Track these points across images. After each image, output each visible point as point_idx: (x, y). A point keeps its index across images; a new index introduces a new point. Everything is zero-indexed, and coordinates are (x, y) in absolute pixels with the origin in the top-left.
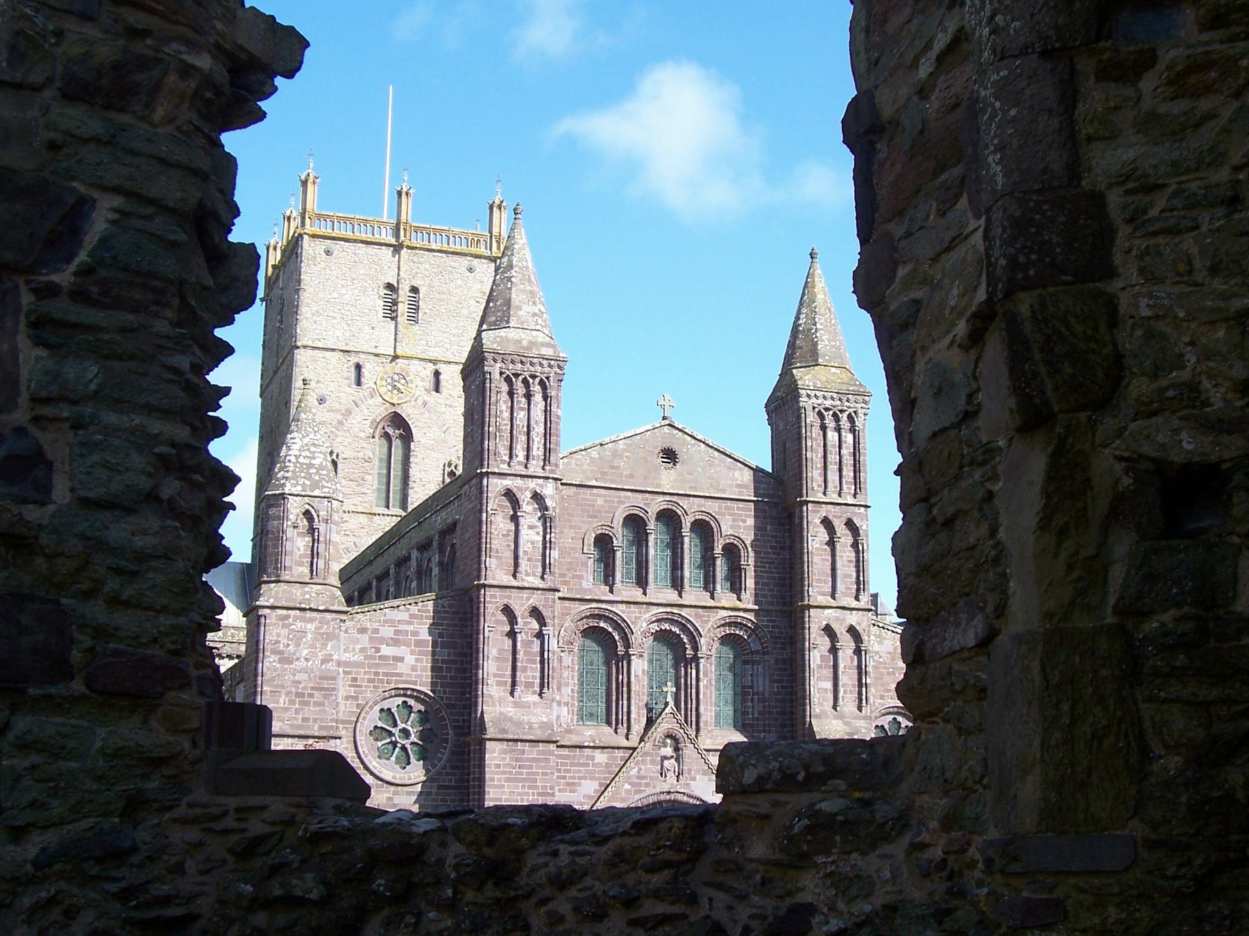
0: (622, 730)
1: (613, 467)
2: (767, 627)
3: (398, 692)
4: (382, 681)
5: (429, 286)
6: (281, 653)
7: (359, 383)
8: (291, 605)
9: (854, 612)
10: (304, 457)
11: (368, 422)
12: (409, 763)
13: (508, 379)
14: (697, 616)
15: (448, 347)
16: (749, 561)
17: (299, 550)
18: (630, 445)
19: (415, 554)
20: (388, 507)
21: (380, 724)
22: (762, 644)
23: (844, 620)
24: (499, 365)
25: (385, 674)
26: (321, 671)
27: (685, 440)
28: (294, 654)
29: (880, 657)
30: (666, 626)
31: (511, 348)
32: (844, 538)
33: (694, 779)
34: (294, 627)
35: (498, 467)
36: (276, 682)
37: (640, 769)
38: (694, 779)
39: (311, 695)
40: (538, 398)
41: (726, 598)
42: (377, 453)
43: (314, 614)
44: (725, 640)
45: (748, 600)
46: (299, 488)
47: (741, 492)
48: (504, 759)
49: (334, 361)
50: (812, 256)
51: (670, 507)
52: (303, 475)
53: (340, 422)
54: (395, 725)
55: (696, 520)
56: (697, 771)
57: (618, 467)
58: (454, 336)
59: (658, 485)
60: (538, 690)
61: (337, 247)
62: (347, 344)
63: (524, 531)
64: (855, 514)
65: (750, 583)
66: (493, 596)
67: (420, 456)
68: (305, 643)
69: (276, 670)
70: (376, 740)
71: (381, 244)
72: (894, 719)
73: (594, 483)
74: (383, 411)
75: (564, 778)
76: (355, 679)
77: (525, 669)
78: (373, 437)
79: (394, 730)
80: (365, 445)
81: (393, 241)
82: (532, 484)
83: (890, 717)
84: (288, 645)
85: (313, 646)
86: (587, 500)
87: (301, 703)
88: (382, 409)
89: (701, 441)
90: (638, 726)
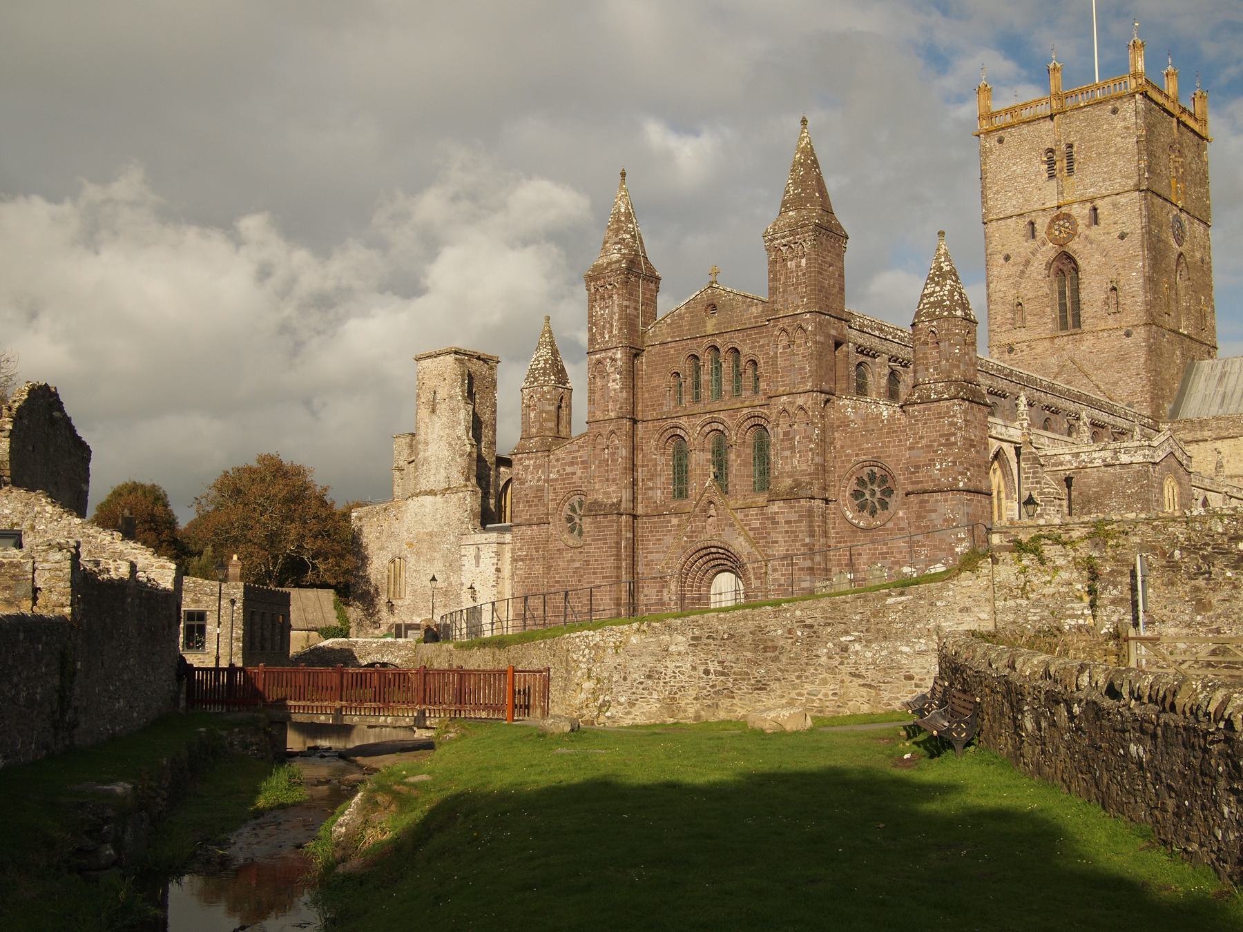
4: (566, 488)
6: (520, 479)
7: (1034, 236)
11: (1044, 265)
33: (723, 530)
37: (692, 526)
38: (723, 530)
49: (1013, 225)
53: (1023, 272)
56: (726, 524)
58: (1105, 173)
61: (1006, 134)
64: (804, 320)
67: (1087, 282)
73: (669, 340)
74: (1052, 254)
75: (655, 536)
78: (1048, 277)
83: (867, 470)
85: (533, 473)
86: (665, 352)
88: (1053, 252)
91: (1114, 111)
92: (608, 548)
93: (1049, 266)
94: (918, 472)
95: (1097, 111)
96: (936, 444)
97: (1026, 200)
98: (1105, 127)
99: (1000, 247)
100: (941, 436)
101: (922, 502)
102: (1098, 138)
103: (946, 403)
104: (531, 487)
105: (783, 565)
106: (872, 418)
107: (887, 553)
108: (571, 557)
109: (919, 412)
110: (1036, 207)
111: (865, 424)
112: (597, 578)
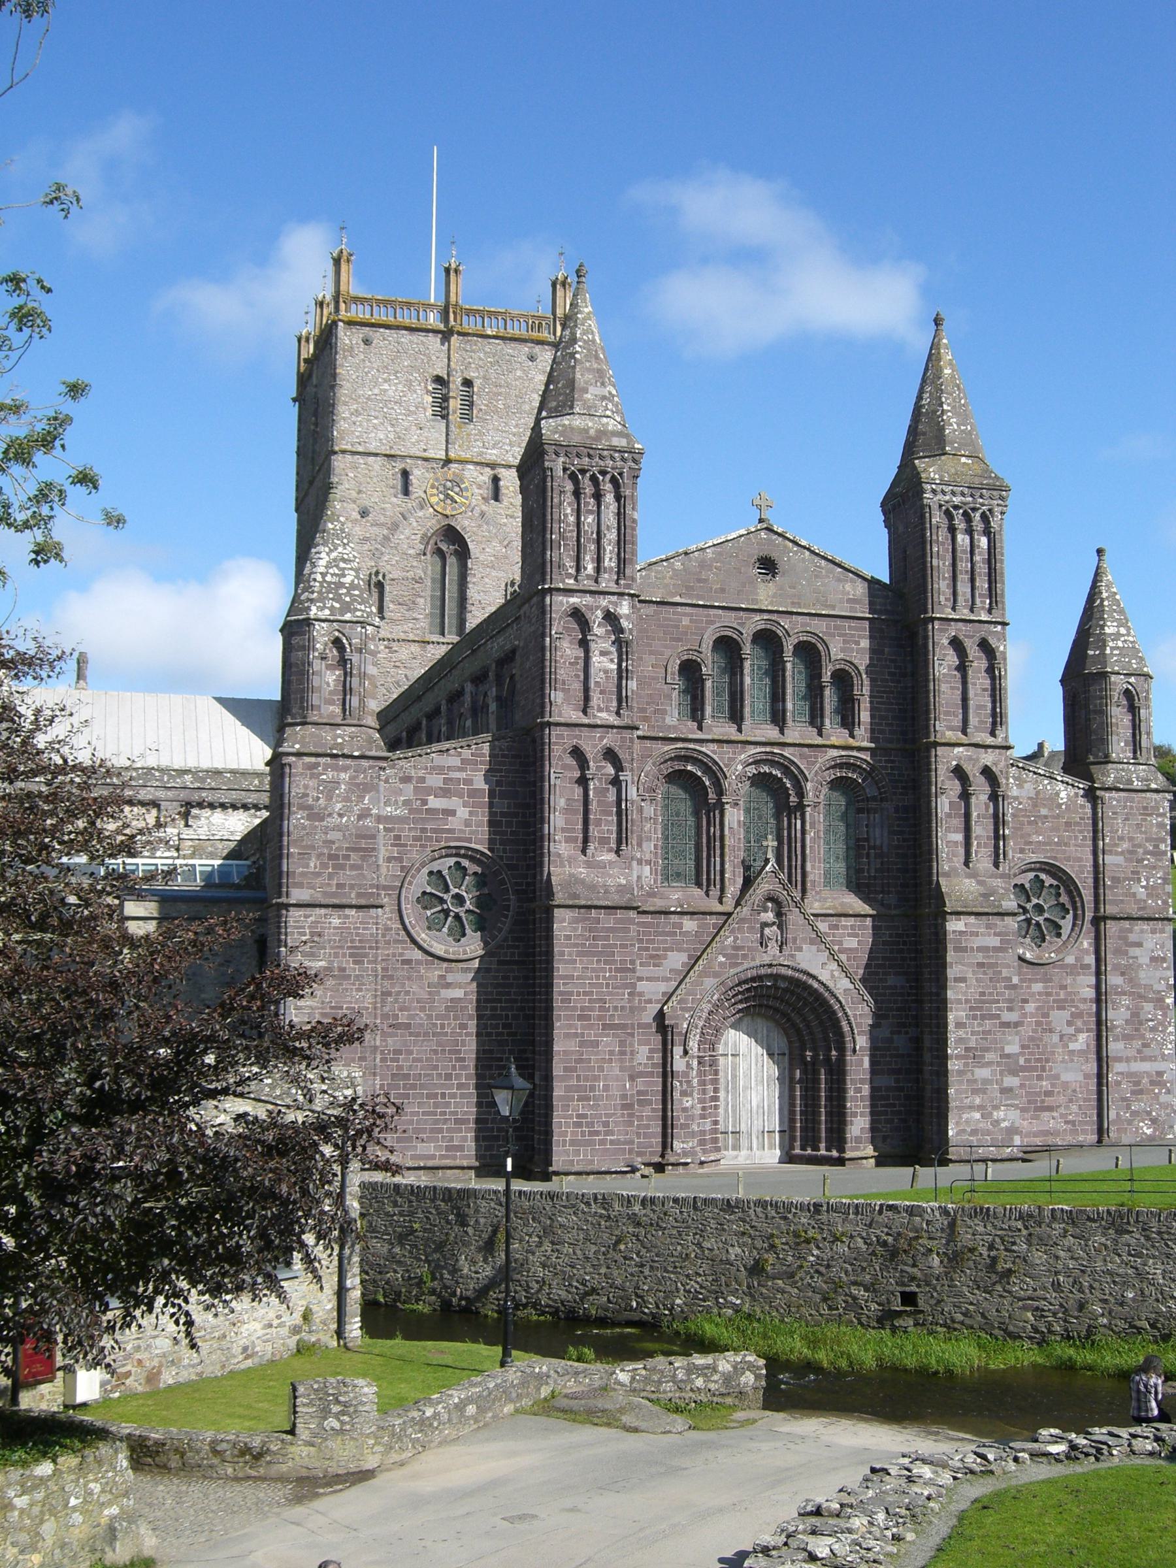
0: (715, 892)
1: (699, 581)
2: (885, 768)
3: (449, 851)
4: (430, 839)
5: (484, 378)
6: (310, 808)
7: (406, 492)
8: (319, 751)
9: (990, 750)
10: (332, 575)
12: (464, 935)
13: (573, 477)
14: (801, 756)
15: (508, 448)
16: (863, 690)
17: (329, 685)
18: (720, 554)
19: (469, 687)
20: (443, 634)
21: (429, 890)
22: (879, 789)
23: (977, 760)
24: (562, 459)
25: (434, 831)
26: (358, 828)
27: (785, 547)
28: (326, 809)
29: (1020, 803)
30: (766, 769)
31: (576, 439)
32: (978, 663)
33: (800, 949)
34: (324, 777)
35: (563, 582)
36: (304, 843)
37: (736, 939)
38: (800, 949)
39: (347, 857)
40: (609, 498)
41: (836, 735)
42: (429, 572)
43: (349, 762)
44: (836, 784)
45: (862, 737)
46: (327, 612)
47: (852, 609)
48: (576, 929)
49: (377, 467)
51: (769, 627)
52: (331, 596)
53: (386, 538)
54: (447, 890)
55: (800, 642)
56: (804, 940)
57: (705, 581)
59: (755, 601)
60: (614, 846)
61: (378, 335)
62: (391, 448)
63: (596, 659)
65: (865, 716)
66: (561, 736)
68: (338, 796)
69: (304, 828)
70: (425, 908)
71: (428, 331)
72: (1037, 876)
73: (677, 599)
75: (647, 949)
76: (398, 838)
77: (598, 823)
78: (425, 554)
79: (445, 896)
80: (415, 564)
81: (442, 327)
82: (604, 602)
83: (1031, 875)
84: (318, 798)
85: (347, 799)
86: (670, 620)
87: (335, 867)
88: (434, 521)
89: (804, 547)
90: (733, 890)
92: (617, 970)
93: (426, 540)
94: (1117, 887)
95: (509, 349)
96: (1141, 850)
97: (399, 438)
98: (519, 373)
99: (354, 494)
100: (1147, 840)
101: (1121, 930)
103: (1155, 796)
104: (338, 828)
105: (975, 1017)
106: (1045, 799)
107: (1065, 1001)
108: (442, 977)
109: (1118, 801)
110: (415, 451)
111: (1035, 805)
112: (590, 1027)
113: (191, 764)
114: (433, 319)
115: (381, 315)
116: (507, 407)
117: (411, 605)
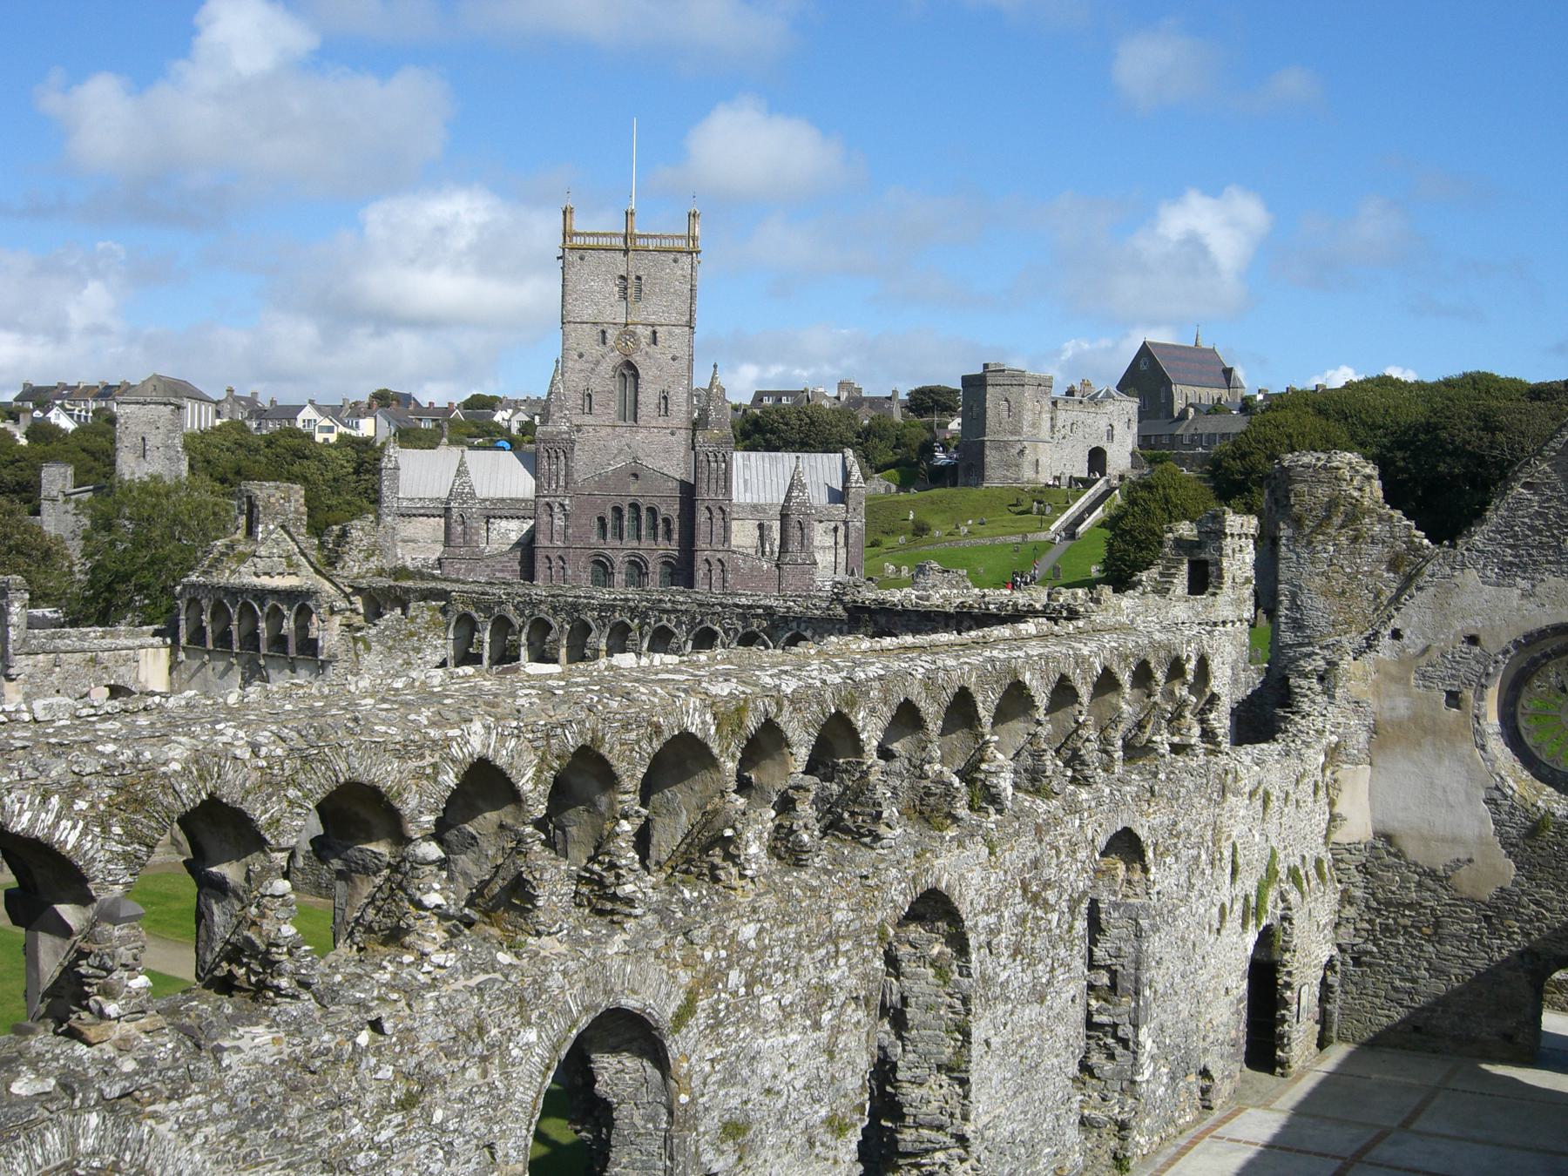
7: (604, 343)
16: (675, 525)
32: (717, 515)
41: (662, 542)
44: (664, 563)
45: (674, 545)
50: (715, 366)
61: (587, 254)
63: (556, 521)
65: (676, 536)
74: (619, 360)
91: (675, 261)
93: (615, 369)
95: (662, 257)
102: (662, 278)
110: (609, 320)
113: (492, 495)
114: (619, 242)
115: (591, 241)
116: (661, 291)
117: (607, 406)
